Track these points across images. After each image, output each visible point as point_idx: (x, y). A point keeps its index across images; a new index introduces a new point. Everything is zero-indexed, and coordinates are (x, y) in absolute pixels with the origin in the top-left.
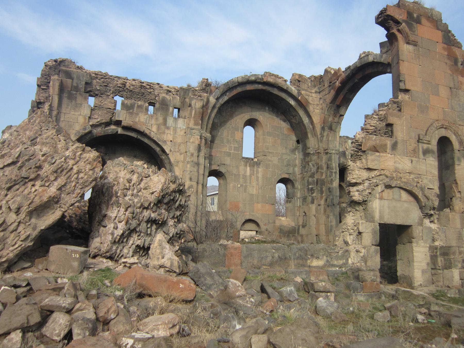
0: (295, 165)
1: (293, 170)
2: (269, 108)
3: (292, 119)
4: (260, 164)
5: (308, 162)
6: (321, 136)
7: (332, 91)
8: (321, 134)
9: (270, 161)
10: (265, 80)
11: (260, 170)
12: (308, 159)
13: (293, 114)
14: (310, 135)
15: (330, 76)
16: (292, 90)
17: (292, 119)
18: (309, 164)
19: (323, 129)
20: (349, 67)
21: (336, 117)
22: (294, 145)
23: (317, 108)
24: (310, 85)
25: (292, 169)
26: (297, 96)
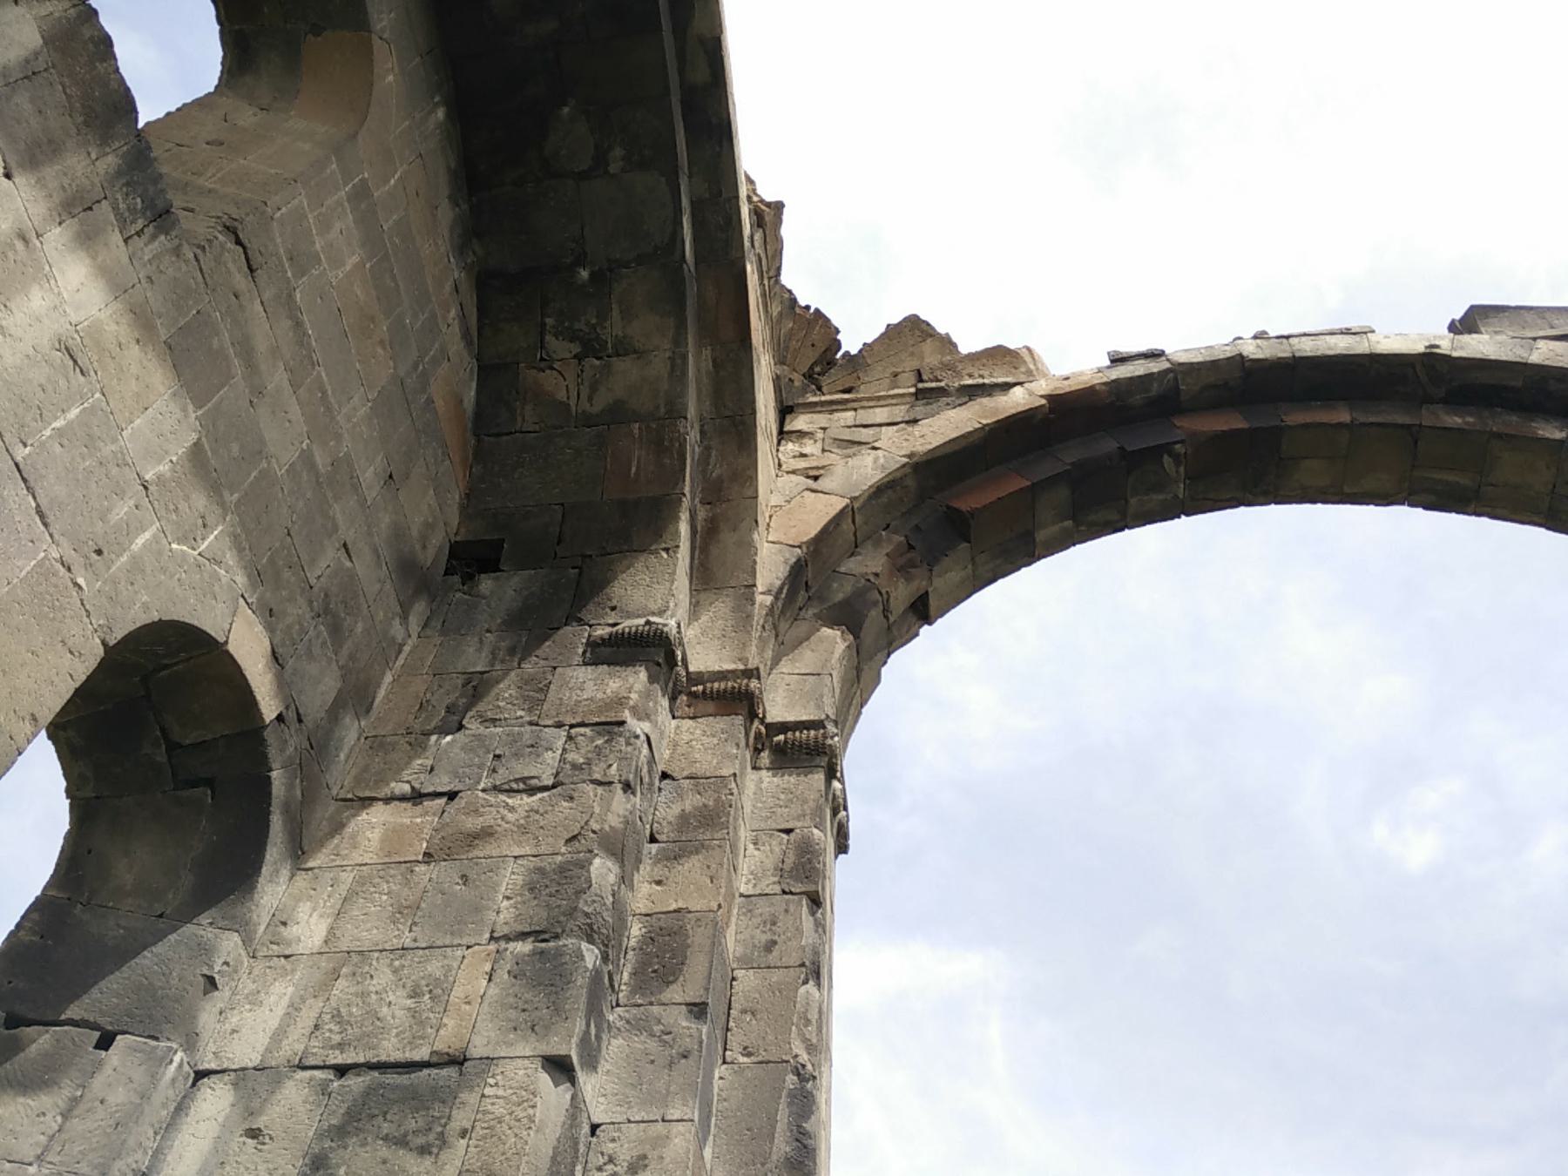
13: (615, 327)
17: (547, 363)
21: (909, 579)
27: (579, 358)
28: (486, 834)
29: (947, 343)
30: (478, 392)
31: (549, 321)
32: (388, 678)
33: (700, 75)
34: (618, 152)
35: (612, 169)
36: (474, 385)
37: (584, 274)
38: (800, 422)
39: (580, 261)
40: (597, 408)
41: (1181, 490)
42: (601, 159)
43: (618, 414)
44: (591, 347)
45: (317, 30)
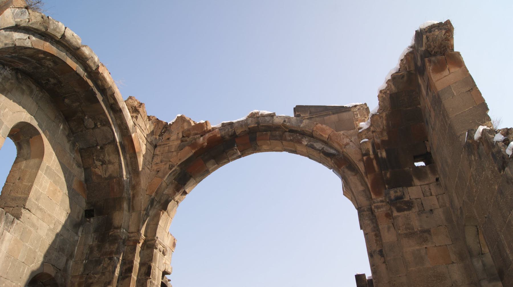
0: (71, 256)
1: (67, 263)
2: (64, 128)
3: (96, 167)
4: (13, 222)
5: (111, 253)
6: (146, 214)
7: (187, 148)
8: (146, 210)
9: (33, 225)
10: (101, 70)
11: (8, 236)
12: (108, 248)
13: (107, 158)
14: (125, 205)
15: (186, 127)
16: (127, 116)
17: (96, 167)
18: (111, 259)
19: (152, 202)
20: (231, 124)
22: (80, 217)
23: (149, 167)
24: (148, 127)
25: (64, 259)
26: (131, 131)
27: (102, 165)
28: (92, 283)
29: (189, 122)
30: (85, 174)
31: (95, 158)
32: (77, 247)
33: (112, 101)
34: (99, 124)
35: (99, 126)
36: (83, 173)
37: (99, 147)
38: (158, 151)
39: (97, 145)
40: (107, 176)
41: (240, 154)
42: (96, 125)
43: (111, 177)
44: (103, 163)
45: (31, 138)
